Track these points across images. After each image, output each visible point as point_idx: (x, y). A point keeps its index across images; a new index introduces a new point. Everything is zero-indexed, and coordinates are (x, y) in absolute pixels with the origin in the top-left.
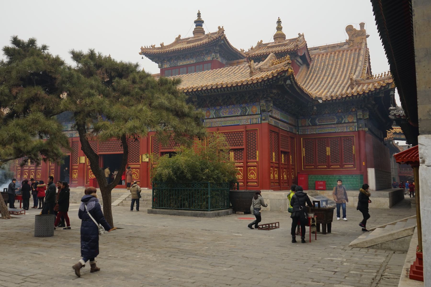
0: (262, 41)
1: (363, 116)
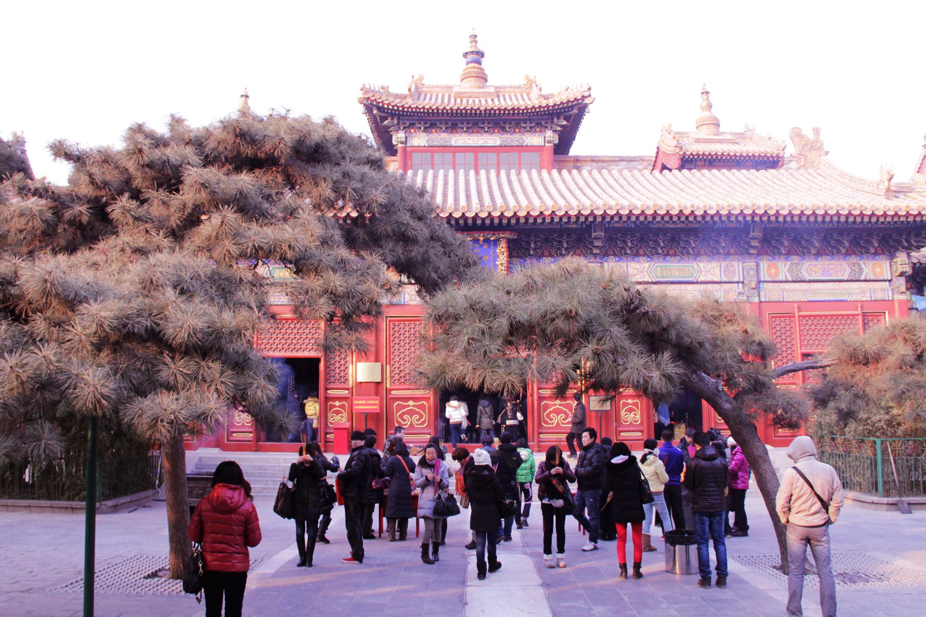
0: (670, 125)
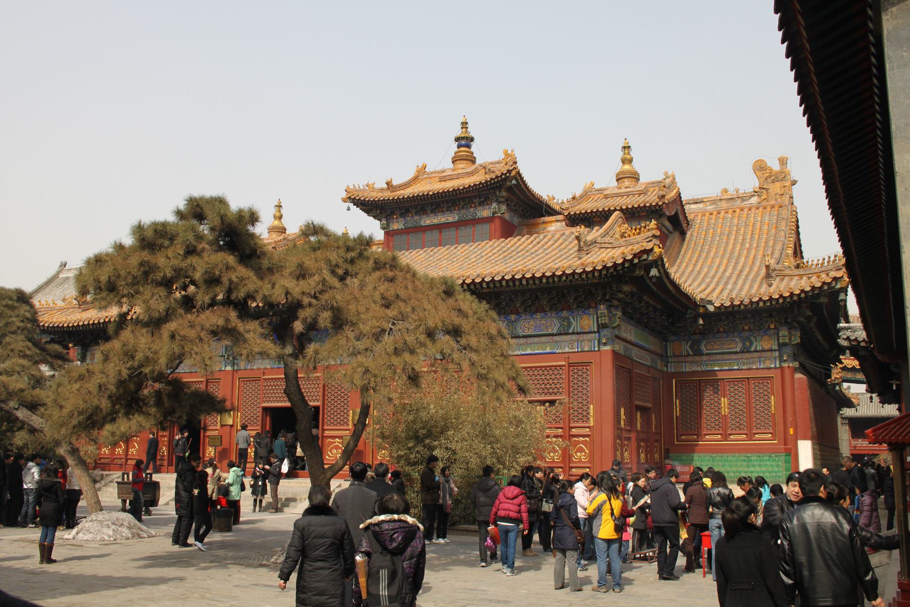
1: (790, 339)
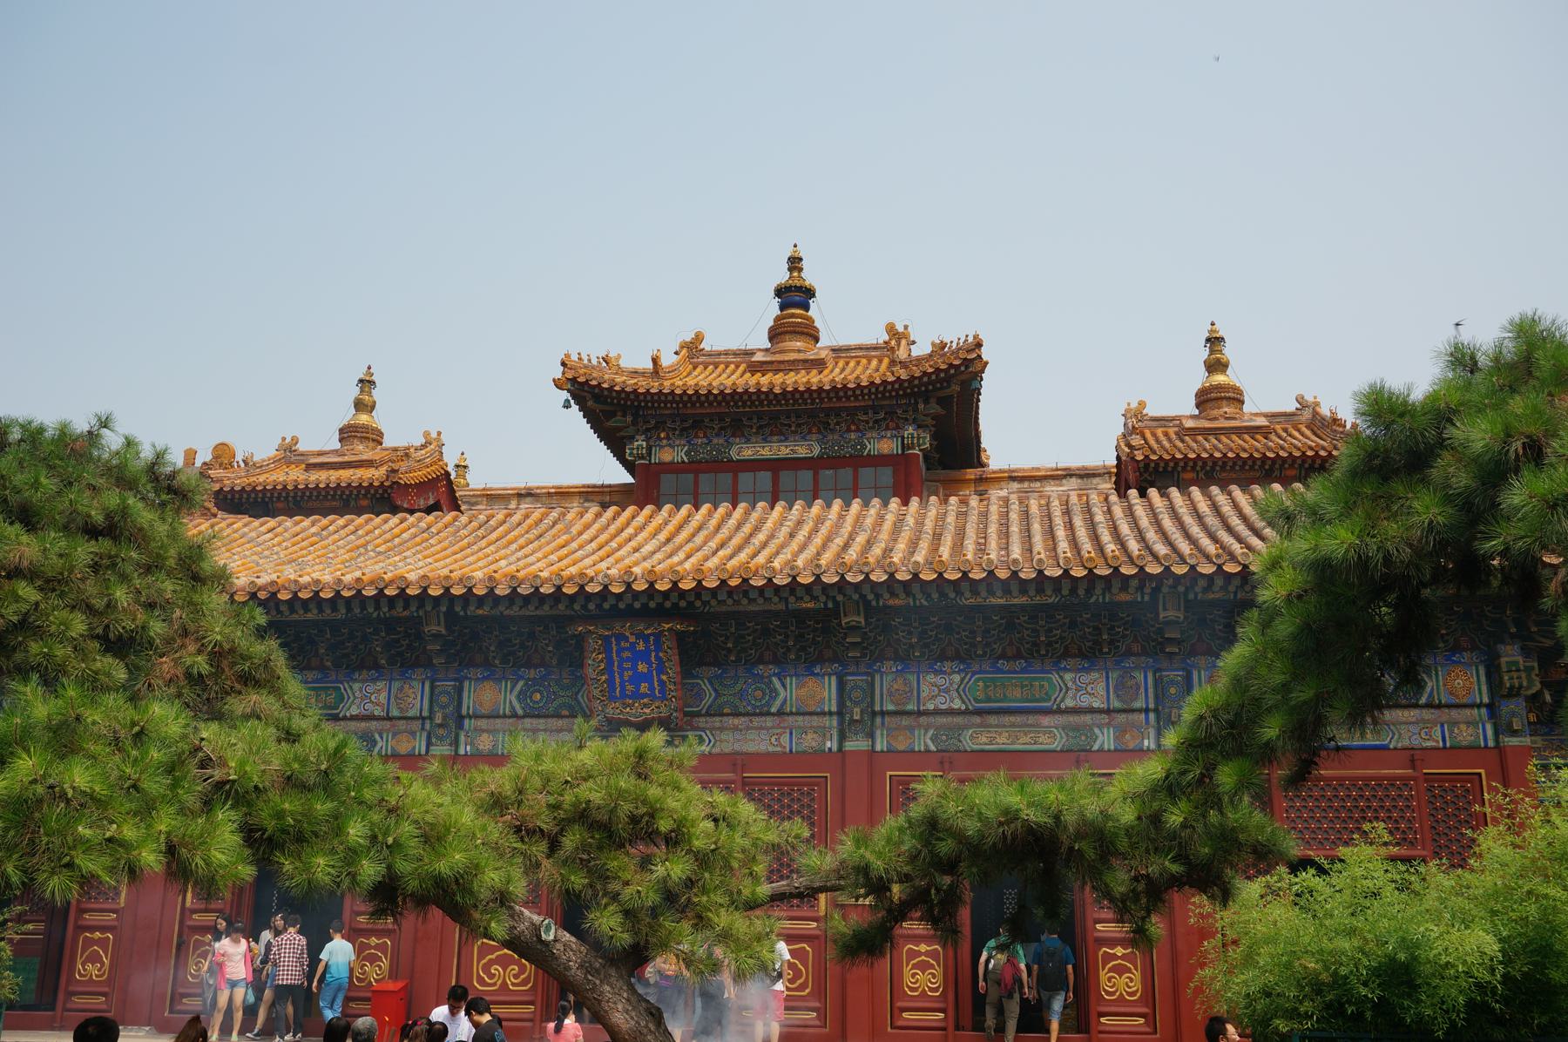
0: (1142, 404)
